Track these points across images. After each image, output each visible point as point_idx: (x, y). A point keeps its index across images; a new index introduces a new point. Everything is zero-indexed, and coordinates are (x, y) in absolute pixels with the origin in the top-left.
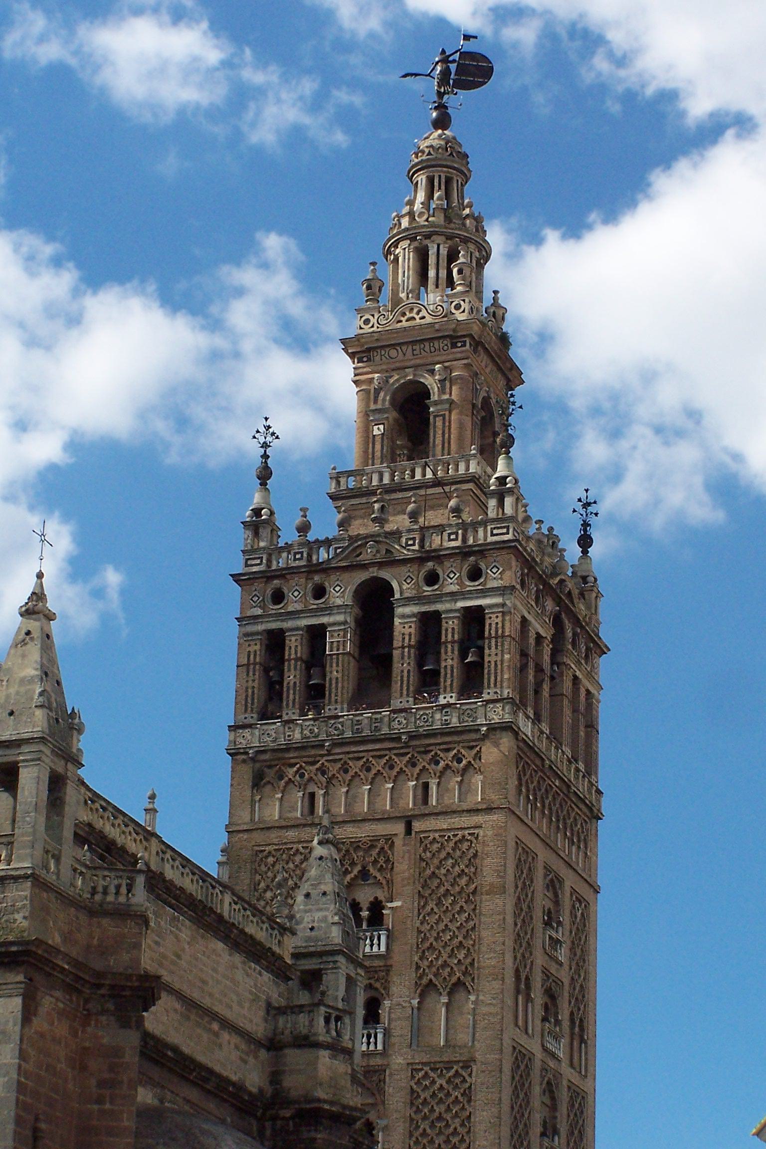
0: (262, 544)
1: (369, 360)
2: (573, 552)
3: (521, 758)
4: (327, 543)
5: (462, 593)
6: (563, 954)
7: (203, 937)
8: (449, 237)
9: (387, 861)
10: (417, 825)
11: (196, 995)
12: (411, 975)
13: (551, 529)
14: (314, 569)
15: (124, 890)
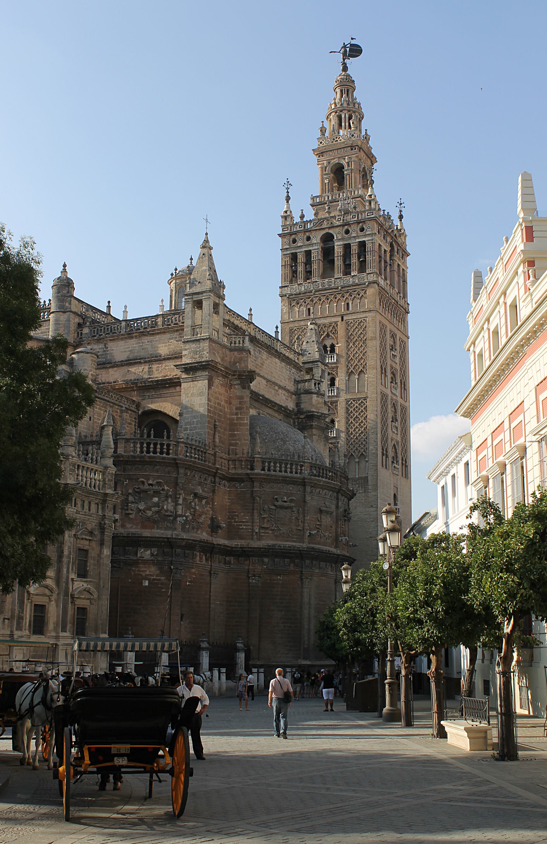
0: (288, 223)
2: (397, 222)
4: (310, 221)
5: (358, 236)
6: (397, 360)
8: (349, 111)
9: (336, 330)
10: (345, 318)
11: (269, 378)
13: (388, 213)
14: (306, 231)
15: (241, 342)
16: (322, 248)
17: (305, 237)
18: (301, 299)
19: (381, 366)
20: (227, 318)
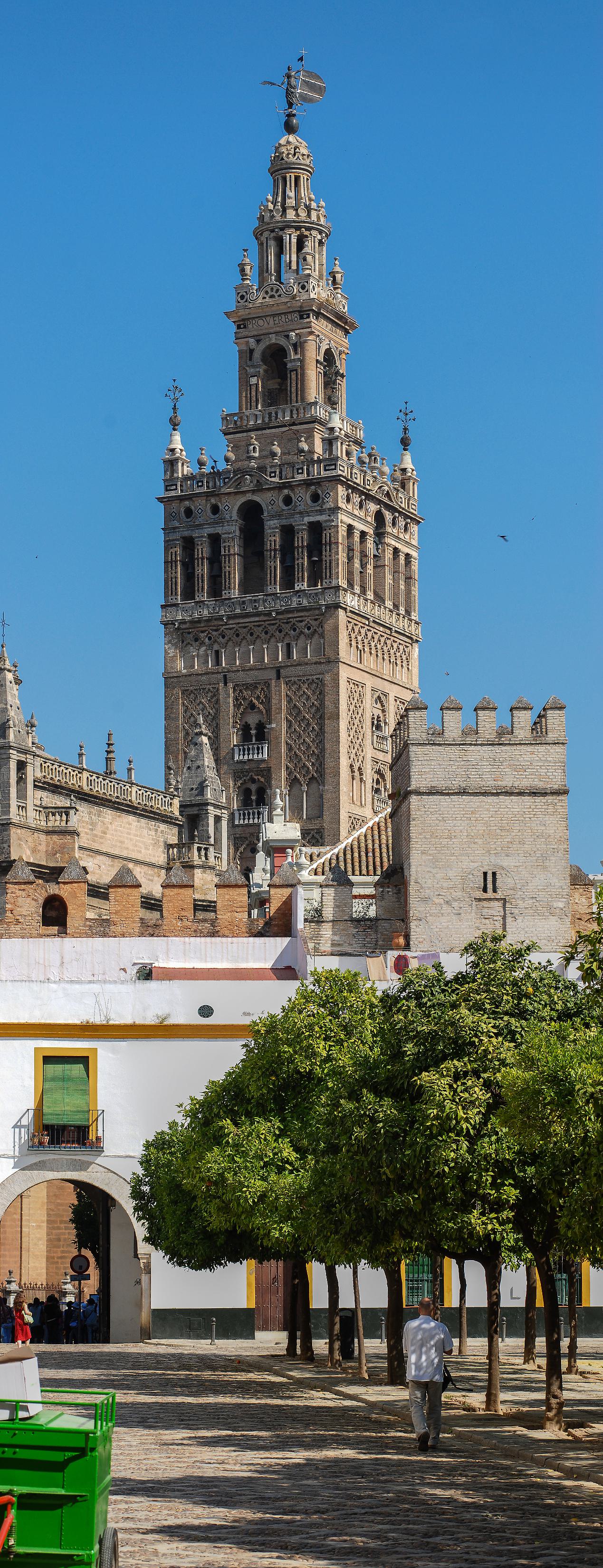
1: (245, 327)
3: (350, 622)
7: (119, 816)
8: (298, 228)
11: (116, 852)
12: (284, 774)
16: (240, 529)
17: (209, 506)
18: (203, 632)
19: (351, 766)
20: (39, 775)
